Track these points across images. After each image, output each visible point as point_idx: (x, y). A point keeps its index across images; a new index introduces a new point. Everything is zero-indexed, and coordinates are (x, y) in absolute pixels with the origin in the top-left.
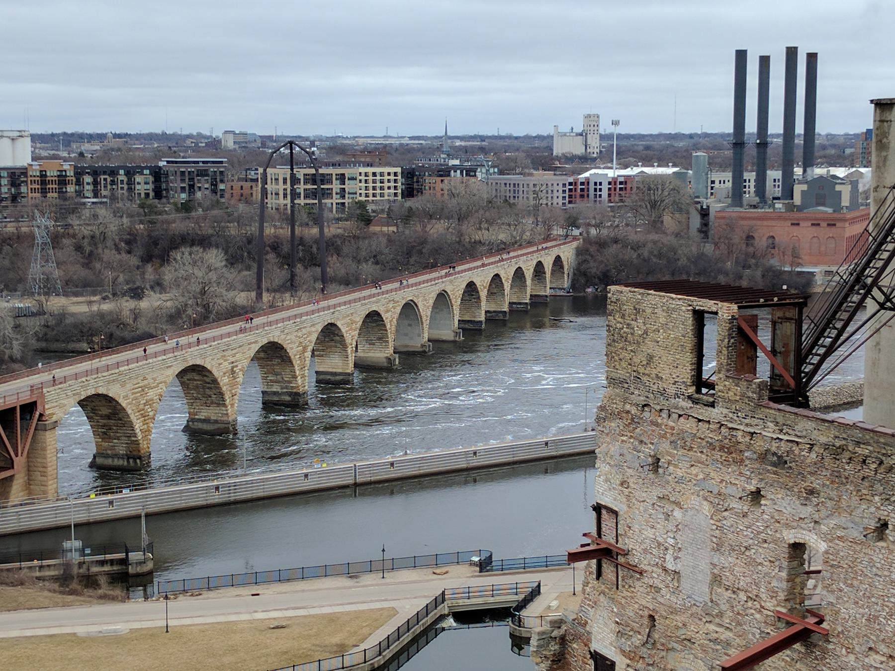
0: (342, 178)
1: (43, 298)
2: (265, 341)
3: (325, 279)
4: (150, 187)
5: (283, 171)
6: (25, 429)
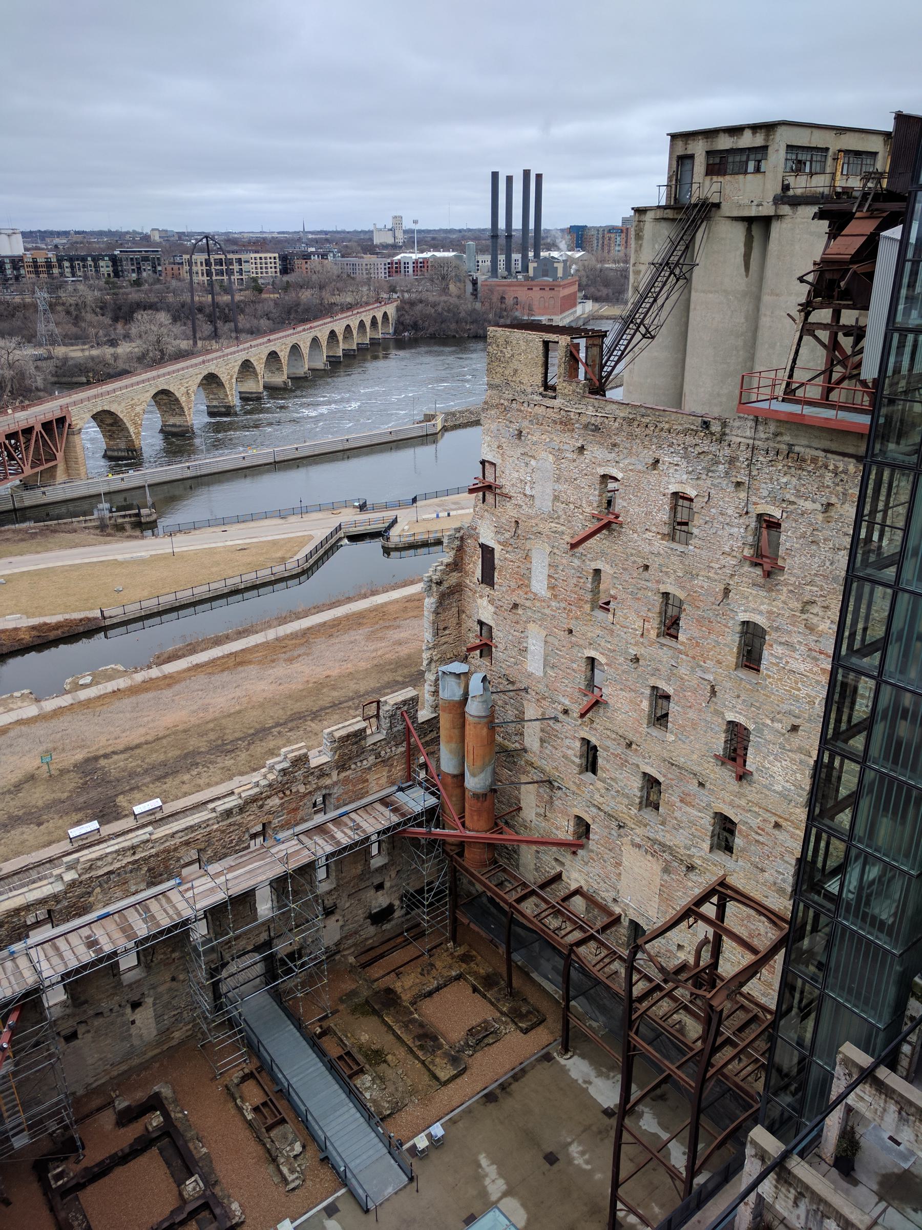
0: (239, 261)
1: (49, 347)
3: (237, 330)
4: (111, 269)
5: (200, 257)
6: (61, 434)
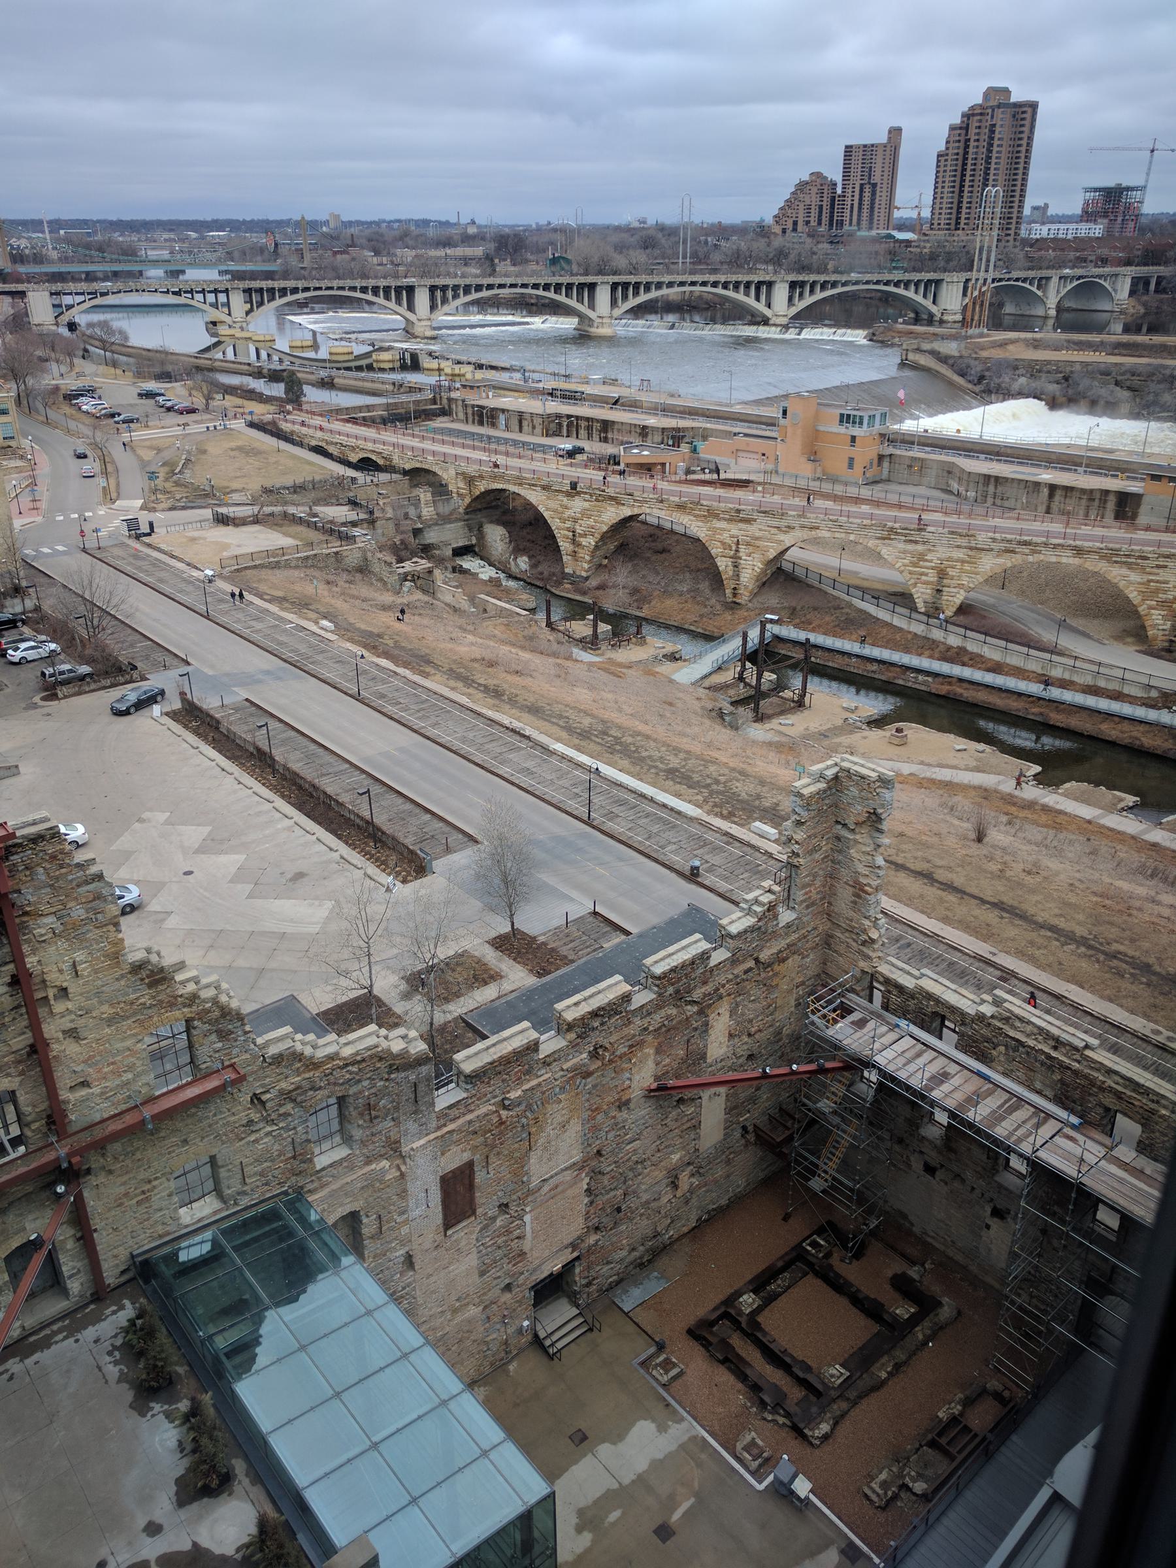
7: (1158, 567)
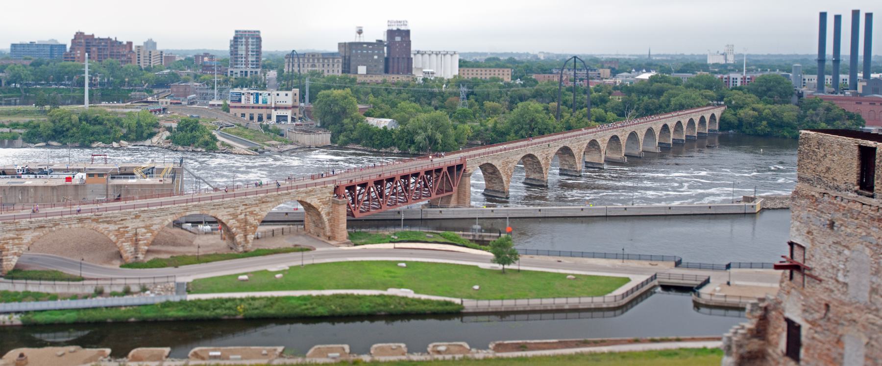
2: (562, 146)
7: (122, 220)
